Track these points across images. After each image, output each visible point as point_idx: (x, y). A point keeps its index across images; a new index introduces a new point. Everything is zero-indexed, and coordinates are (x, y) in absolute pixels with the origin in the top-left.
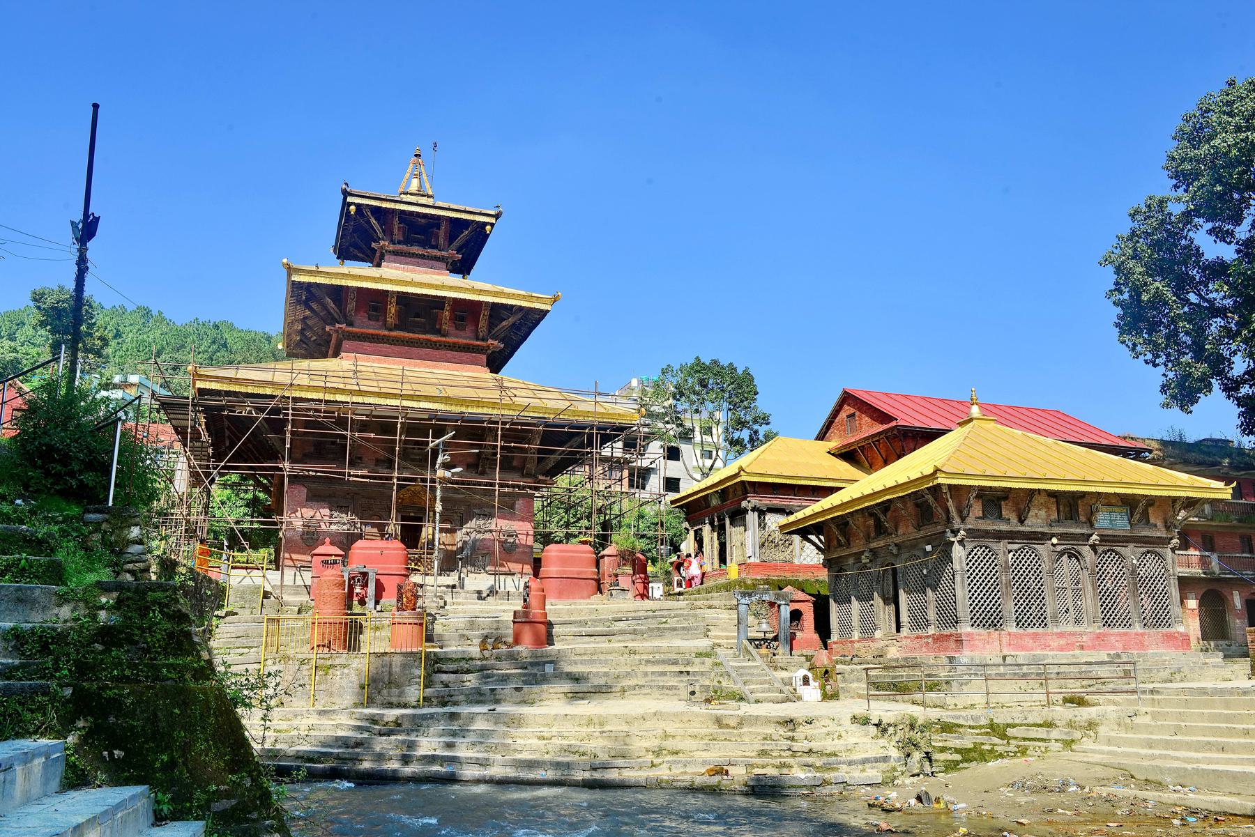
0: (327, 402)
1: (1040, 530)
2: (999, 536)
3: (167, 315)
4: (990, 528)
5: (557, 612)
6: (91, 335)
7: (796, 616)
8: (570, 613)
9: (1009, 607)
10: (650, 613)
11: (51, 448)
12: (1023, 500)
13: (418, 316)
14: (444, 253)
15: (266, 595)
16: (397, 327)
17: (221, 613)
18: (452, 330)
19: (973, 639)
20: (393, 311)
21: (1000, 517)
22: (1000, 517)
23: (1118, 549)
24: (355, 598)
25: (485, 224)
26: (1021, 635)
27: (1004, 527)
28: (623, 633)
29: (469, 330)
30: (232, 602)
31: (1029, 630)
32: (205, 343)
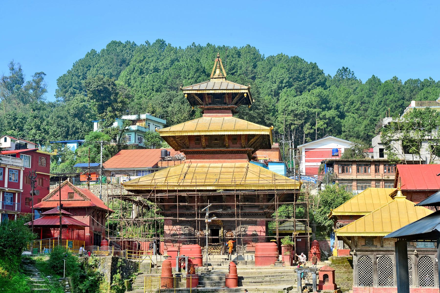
0: (170, 191)
1: (390, 249)
2: (372, 251)
3: (173, 45)
4: (368, 249)
5: (247, 273)
6: (116, 102)
7: (326, 276)
8: (252, 273)
9: (376, 278)
10: (280, 274)
11: (55, 265)
12: (381, 239)
13: (216, 140)
14: (229, 106)
15: (153, 266)
16: (207, 146)
17: (136, 274)
18: (231, 144)
19: (358, 290)
20: (204, 141)
21: (373, 244)
22: (373, 244)
23: (430, 256)
24: (182, 267)
25: (244, 93)
26: (379, 289)
27: (374, 249)
28: (266, 282)
29: (238, 145)
30: (141, 269)
31: (384, 287)
32: (192, 72)
